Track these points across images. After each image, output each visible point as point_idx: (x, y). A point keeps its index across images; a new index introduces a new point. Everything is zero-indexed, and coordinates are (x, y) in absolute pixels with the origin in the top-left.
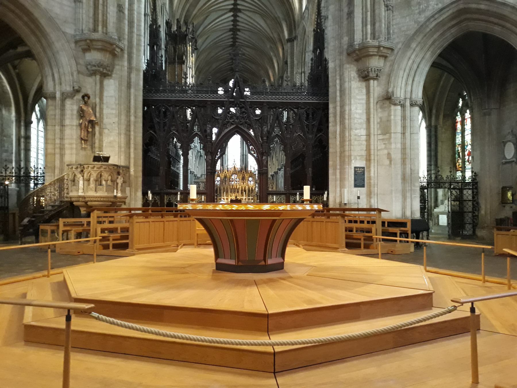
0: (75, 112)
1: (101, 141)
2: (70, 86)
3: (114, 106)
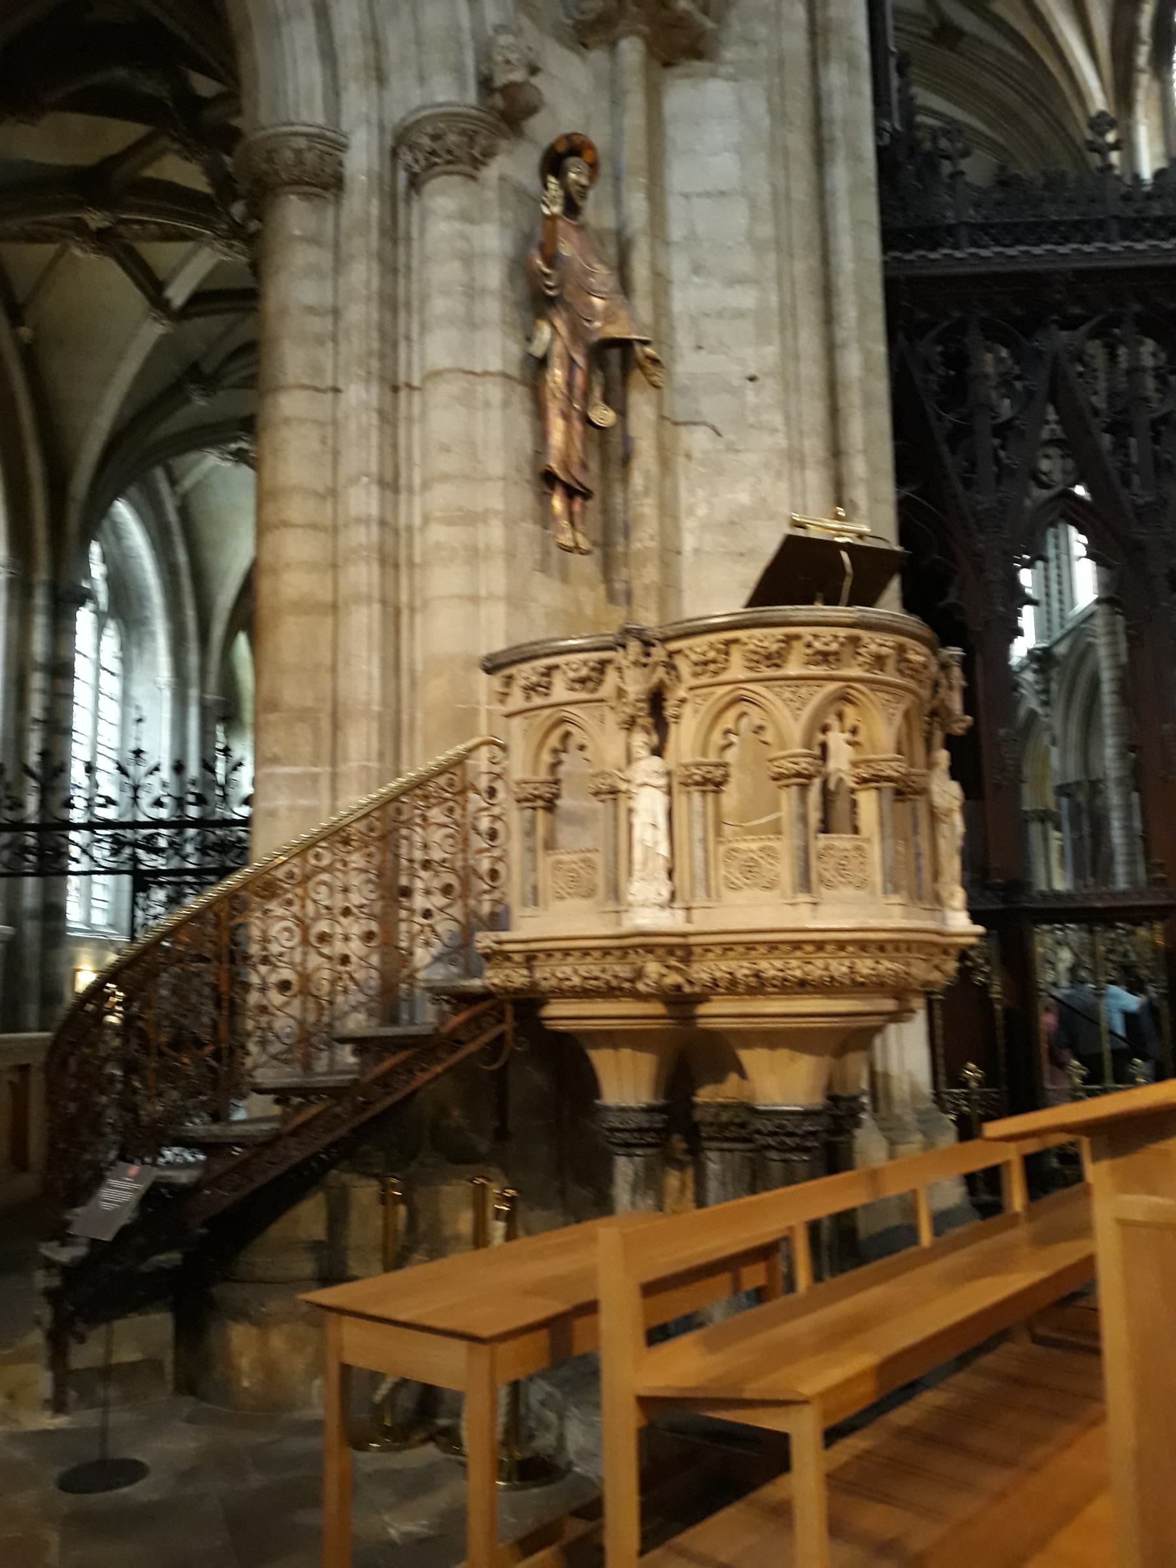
0: (493, 276)
1: (669, 511)
2: (458, 70)
3: (744, 262)
